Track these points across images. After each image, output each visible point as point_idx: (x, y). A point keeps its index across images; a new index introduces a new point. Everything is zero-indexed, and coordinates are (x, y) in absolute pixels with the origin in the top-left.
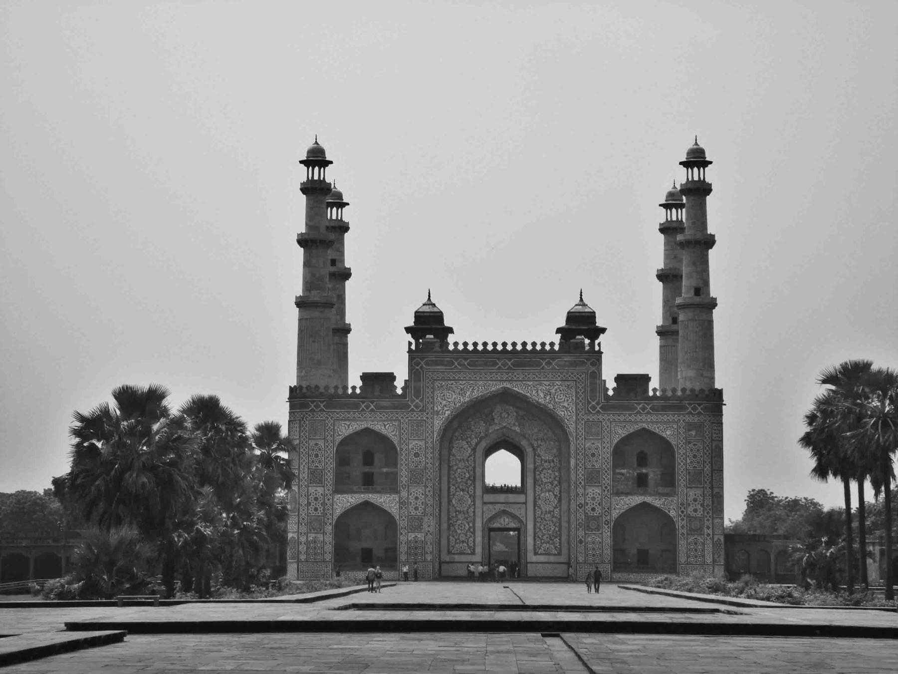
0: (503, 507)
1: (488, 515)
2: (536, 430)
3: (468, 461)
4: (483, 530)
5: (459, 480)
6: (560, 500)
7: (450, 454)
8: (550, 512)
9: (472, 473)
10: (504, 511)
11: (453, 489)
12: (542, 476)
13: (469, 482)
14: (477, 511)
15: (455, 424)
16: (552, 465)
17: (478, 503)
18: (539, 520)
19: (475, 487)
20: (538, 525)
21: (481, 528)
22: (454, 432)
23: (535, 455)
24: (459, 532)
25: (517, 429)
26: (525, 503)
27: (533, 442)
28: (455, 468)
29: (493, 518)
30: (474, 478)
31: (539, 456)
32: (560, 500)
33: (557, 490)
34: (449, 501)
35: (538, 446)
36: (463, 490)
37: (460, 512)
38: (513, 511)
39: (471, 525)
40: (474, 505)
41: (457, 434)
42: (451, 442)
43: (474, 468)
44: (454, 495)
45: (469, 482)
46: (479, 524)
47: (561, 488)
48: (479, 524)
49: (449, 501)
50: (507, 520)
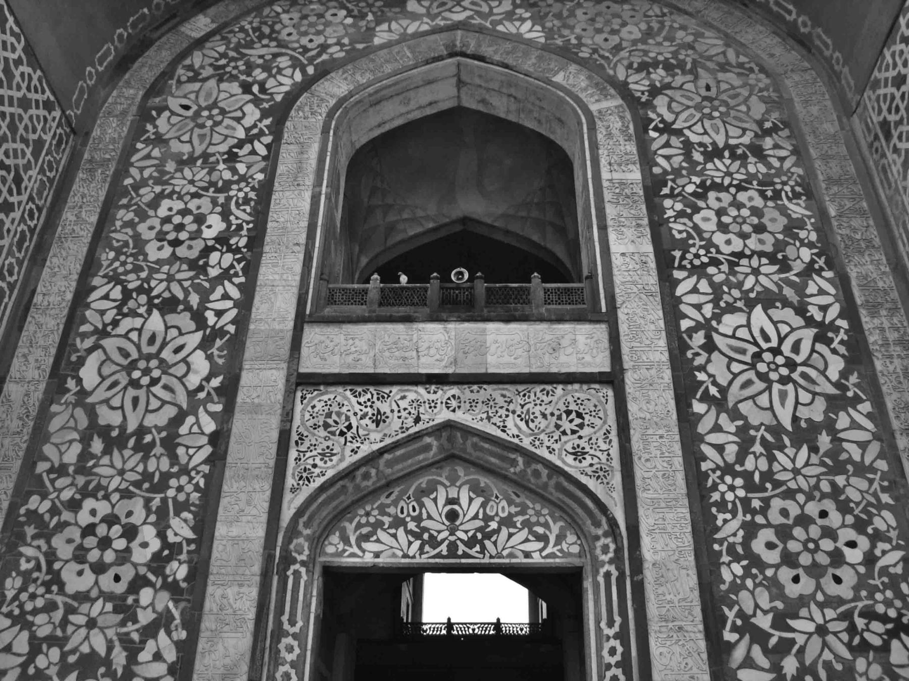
0: (440, 408)
1: (323, 461)
2: (632, 32)
3: (232, 158)
4: (274, 565)
5: (154, 252)
6: (858, 354)
7: (137, 132)
8: (804, 434)
9: (241, 215)
10: (449, 426)
11: (103, 300)
12: (706, 220)
13: (219, 260)
14: (239, 424)
15: (201, 24)
16: (754, 167)
17: (263, 381)
18: (729, 490)
19: (248, 290)
20: (730, 528)
21: (257, 568)
22: (186, 53)
23: (643, 125)
24: (77, 580)
25: (528, 30)
26: (613, 379)
27: (621, 74)
28: (147, 194)
29: (352, 494)
30: (257, 240)
31: (667, 128)
32: (858, 354)
33: (822, 293)
34: (64, 365)
35: (655, 91)
36: (169, 306)
37: (115, 441)
38: (514, 429)
39: (181, 529)
40: (229, 391)
41: (197, 59)
42: (157, 88)
43: (265, 191)
44: (103, 333)
45: (219, 260)
46: (241, 526)
47: (843, 282)
48: (241, 526)
49: (64, 365)
50: (470, 508)
